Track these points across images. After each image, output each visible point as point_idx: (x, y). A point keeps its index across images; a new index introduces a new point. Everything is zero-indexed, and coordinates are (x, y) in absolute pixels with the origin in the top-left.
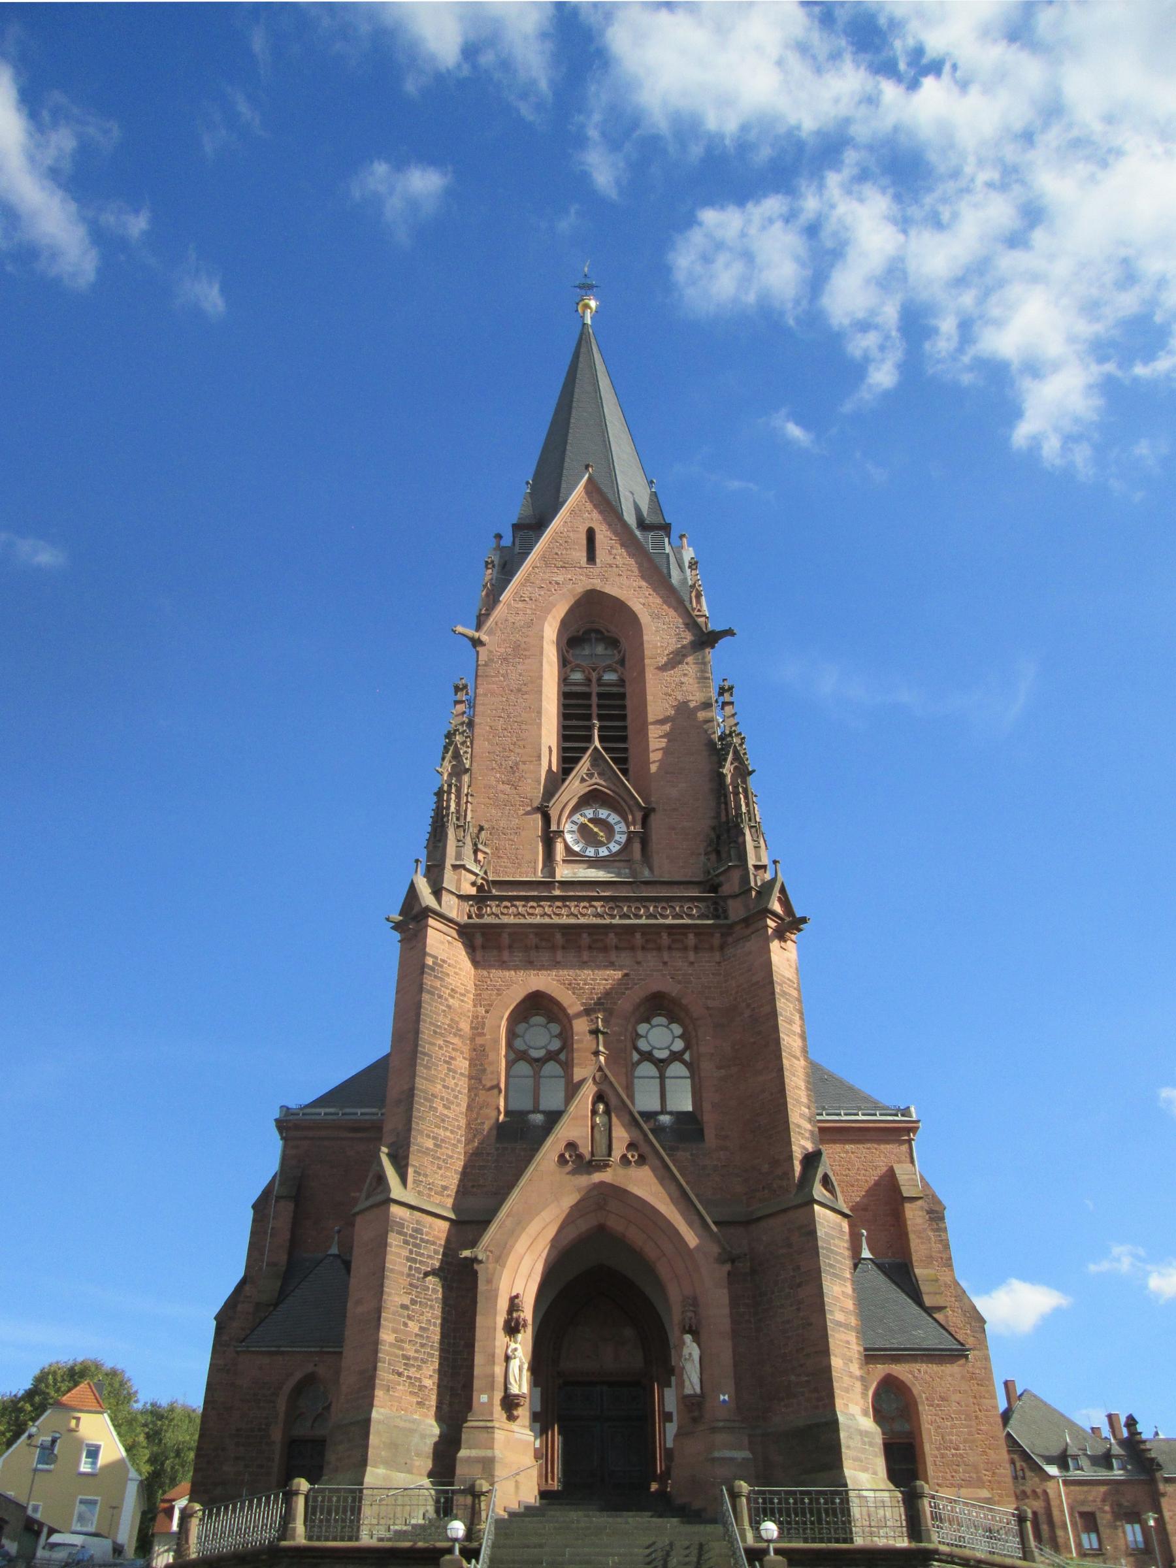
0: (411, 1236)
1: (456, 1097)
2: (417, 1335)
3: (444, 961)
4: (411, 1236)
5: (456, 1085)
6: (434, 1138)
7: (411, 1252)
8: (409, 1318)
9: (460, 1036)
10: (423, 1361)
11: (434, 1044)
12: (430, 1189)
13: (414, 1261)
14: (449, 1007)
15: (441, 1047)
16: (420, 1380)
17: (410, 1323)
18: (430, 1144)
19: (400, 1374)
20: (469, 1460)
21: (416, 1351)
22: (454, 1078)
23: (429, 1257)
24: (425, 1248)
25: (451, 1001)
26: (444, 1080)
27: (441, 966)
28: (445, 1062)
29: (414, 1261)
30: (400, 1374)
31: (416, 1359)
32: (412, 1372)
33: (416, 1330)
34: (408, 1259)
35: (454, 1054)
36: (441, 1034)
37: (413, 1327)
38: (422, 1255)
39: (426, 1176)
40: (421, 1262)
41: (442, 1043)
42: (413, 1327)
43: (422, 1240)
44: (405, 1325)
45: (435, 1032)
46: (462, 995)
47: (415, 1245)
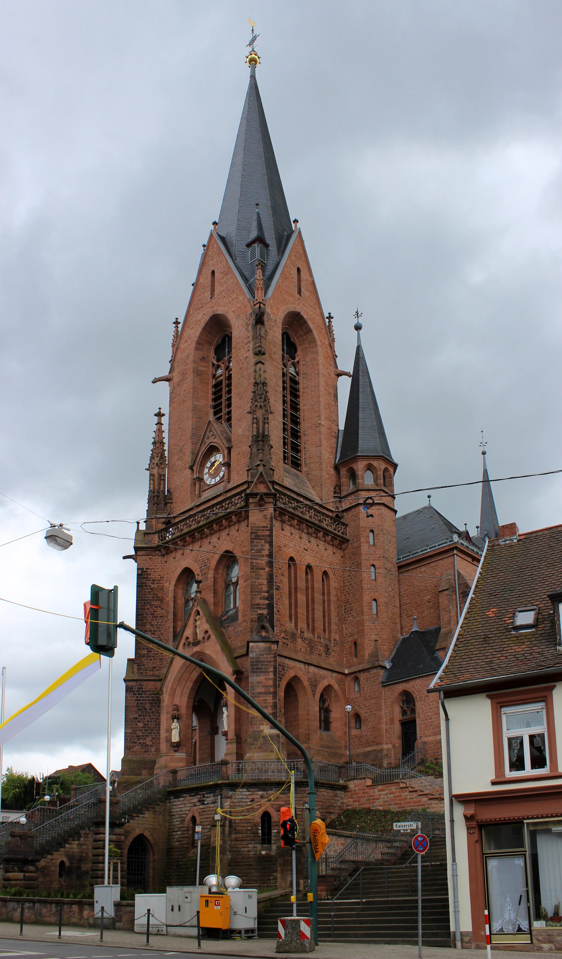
0: (137, 691)
1: (158, 628)
2: (142, 727)
3: (148, 569)
4: (137, 691)
5: (158, 622)
6: (147, 649)
7: (137, 697)
8: (138, 722)
9: (159, 600)
10: (146, 736)
11: (145, 609)
12: (147, 670)
13: (139, 700)
14: (152, 589)
15: (148, 609)
16: (145, 743)
17: (139, 724)
18: (145, 652)
19: (135, 743)
20: (158, 768)
21: (143, 733)
22: (156, 620)
23: (148, 697)
24: (144, 694)
25: (152, 586)
26: (151, 623)
27: (146, 572)
28: (151, 614)
29: (139, 700)
30: (135, 743)
31: (142, 736)
32: (141, 741)
33: (142, 726)
34: (136, 700)
35: (156, 609)
36: (148, 603)
37: (140, 725)
38: (144, 697)
39: (144, 665)
40: (142, 700)
41: (149, 607)
42: (140, 725)
43: (143, 691)
44: (137, 725)
45: (145, 603)
46: (158, 580)
47: (139, 694)
